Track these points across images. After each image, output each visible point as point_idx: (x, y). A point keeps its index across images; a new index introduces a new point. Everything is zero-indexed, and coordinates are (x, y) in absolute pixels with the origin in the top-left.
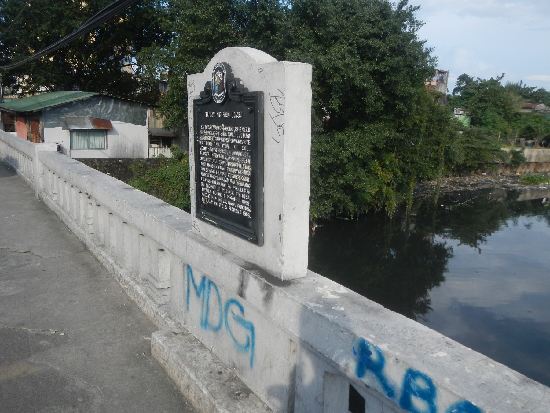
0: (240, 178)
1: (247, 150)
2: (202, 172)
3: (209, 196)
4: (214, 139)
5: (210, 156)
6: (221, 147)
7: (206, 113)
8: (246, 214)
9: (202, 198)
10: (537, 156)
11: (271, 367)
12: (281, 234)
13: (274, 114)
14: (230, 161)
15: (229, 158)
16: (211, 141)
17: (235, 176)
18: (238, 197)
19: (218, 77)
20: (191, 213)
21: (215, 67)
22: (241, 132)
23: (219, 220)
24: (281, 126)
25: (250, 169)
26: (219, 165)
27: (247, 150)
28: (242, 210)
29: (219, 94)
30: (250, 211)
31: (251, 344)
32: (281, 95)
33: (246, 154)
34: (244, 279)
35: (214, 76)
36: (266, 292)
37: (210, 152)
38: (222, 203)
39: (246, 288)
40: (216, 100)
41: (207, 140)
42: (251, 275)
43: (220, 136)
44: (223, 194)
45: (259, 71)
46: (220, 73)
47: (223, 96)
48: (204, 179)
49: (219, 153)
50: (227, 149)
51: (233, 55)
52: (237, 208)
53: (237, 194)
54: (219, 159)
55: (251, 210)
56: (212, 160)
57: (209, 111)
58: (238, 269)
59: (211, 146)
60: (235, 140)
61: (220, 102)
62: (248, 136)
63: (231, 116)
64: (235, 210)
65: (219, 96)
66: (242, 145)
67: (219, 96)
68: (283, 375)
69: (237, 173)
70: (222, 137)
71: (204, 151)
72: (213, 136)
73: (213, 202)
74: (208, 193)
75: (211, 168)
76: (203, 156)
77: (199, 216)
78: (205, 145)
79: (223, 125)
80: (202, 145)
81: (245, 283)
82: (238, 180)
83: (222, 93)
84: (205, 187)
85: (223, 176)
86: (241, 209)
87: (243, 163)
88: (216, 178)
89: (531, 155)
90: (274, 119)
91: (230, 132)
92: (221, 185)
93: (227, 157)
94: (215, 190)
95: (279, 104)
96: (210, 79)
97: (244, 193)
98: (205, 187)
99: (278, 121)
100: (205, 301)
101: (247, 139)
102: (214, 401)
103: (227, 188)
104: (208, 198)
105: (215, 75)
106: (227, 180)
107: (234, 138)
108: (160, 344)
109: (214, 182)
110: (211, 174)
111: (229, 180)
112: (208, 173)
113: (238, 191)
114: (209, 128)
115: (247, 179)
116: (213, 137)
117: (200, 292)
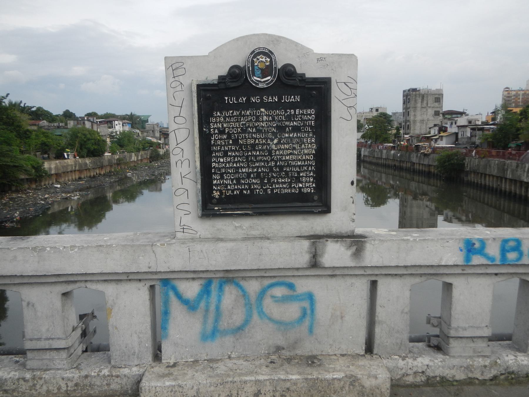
0: (294, 157)
1: (310, 130)
3: (229, 187)
6: (259, 131)
8: (305, 191)
9: (214, 192)
10: (56, 168)
11: (342, 317)
12: (354, 197)
13: (342, 97)
15: (275, 141)
16: (237, 128)
17: (287, 158)
18: (294, 177)
19: (262, 61)
21: (253, 51)
22: (298, 115)
23: (252, 208)
24: (353, 107)
25: (315, 147)
26: (257, 151)
28: (300, 188)
29: (262, 78)
30: (314, 185)
31: (309, 312)
32: (352, 81)
34: (317, 248)
35: (253, 62)
36: (354, 249)
37: (233, 140)
39: (322, 255)
41: (229, 128)
42: (329, 242)
44: (262, 180)
45: (320, 59)
46: (264, 57)
47: (272, 81)
48: (220, 171)
49: (255, 139)
50: (273, 133)
51: (272, 41)
52: (290, 187)
54: (253, 146)
55: (315, 184)
58: (306, 244)
63: (280, 99)
68: (360, 315)
69: (291, 154)
70: (263, 121)
72: (241, 122)
81: (319, 252)
83: (269, 78)
84: (222, 178)
85: (264, 161)
87: (301, 143)
88: (248, 165)
89: (51, 167)
90: (342, 101)
93: (272, 140)
94: (243, 179)
95: (350, 88)
99: (349, 103)
100: (212, 308)
101: (312, 120)
102: (314, 376)
105: (255, 60)
107: (286, 121)
108: (169, 387)
109: (244, 170)
110: (239, 161)
112: (229, 162)
114: (233, 113)
115: (311, 157)
117: (198, 304)
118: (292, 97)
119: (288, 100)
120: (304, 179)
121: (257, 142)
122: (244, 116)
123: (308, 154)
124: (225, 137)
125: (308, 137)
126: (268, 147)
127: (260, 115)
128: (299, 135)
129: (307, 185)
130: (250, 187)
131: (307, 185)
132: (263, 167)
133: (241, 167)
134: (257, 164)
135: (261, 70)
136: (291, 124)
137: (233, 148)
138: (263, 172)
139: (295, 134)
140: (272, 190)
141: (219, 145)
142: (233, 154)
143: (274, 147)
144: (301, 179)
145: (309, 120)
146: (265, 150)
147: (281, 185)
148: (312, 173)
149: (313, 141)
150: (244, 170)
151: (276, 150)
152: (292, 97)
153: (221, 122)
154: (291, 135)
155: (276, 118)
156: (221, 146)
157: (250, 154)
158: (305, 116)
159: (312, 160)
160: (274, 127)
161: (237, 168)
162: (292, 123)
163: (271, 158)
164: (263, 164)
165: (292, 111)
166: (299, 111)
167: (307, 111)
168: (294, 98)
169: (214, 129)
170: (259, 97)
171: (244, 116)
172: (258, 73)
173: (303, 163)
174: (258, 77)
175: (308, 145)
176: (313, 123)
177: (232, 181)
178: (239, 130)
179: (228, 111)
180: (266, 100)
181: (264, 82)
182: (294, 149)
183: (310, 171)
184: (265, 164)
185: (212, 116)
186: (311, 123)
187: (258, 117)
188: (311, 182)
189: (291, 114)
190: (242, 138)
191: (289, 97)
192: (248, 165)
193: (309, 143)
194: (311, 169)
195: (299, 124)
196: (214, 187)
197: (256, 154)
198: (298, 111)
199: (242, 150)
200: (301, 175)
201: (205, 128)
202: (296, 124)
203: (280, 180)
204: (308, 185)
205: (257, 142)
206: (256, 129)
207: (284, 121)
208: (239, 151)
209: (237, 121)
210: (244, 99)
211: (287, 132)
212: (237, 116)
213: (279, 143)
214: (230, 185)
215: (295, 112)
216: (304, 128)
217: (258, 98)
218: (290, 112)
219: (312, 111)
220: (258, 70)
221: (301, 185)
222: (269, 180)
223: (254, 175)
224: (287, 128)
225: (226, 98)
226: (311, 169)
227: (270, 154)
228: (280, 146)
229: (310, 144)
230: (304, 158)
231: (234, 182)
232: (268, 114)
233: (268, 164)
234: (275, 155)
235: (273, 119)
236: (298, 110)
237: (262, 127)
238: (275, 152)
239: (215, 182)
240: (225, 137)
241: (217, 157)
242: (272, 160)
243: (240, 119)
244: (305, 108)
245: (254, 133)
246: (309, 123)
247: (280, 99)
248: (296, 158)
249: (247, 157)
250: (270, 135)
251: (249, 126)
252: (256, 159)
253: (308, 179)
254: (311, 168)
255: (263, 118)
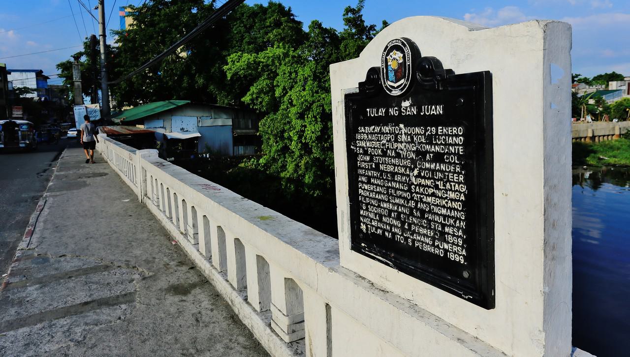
0: (438, 201)
1: (456, 162)
2: (360, 190)
3: (373, 224)
4: (384, 145)
5: (377, 168)
6: (398, 155)
7: (368, 110)
8: (452, 257)
9: (362, 224)
14: (419, 176)
15: (416, 172)
16: (377, 148)
17: (429, 199)
20: (337, 238)
22: (442, 135)
25: (464, 190)
26: (396, 181)
27: (456, 162)
28: (446, 251)
29: (396, 83)
30: (464, 253)
33: (455, 167)
35: (386, 59)
38: (402, 235)
40: (391, 91)
41: (371, 148)
43: (396, 141)
44: (403, 223)
47: (405, 85)
48: (365, 200)
49: (395, 165)
52: (433, 245)
53: (435, 225)
54: (393, 174)
56: (381, 175)
57: (370, 108)
59: (378, 155)
60: (428, 147)
61: (399, 94)
62: (460, 140)
64: (427, 248)
65: (396, 85)
66: (444, 154)
67: (395, 87)
69: (433, 195)
70: (401, 142)
71: (365, 161)
72: (381, 141)
73: (384, 233)
74: (373, 219)
75: (377, 185)
76: (362, 168)
77: (356, 247)
78: (366, 153)
79: (402, 126)
80: (361, 154)
82: (437, 205)
83: (402, 81)
84: (367, 209)
85: (405, 198)
86: (444, 249)
88: (389, 199)
91: (417, 134)
92: (400, 210)
93: (412, 170)
94: (385, 216)
96: (378, 63)
97: (450, 226)
98: (367, 209)
101: (459, 145)
103: (411, 214)
104: (370, 223)
106: (412, 204)
107: (426, 144)
109: (385, 205)
110: (379, 193)
111: (417, 204)
112: (372, 191)
113: (435, 221)
114: (374, 130)
116: (382, 143)
118: (433, 107)
119: (428, 112)
120: (450, 238)
121: (396, 170)
122: (383, 134)
123: (455, 200)
124: (368, 158)
125: (455, 172)
126: (408, 180)
127: (398, 134)
128: (442, 167)
129: (455, 249)
130: (391, 229)
131: (455, 249)
132: (404, 206)
133: (384, 201)
134: (397, 201)
135: (394, 70)
136: (432, 150)
137: (375, 175)
138: (403, 213)
139: (438, 164)
140: (413, 241)
141: (362, 168)
142: (376, 182)
143: (413, 179)
144: (446, 236)
145: (456, 144)
146: (404, 183)
147: (422, 237)
148: (460, 231)
149: (461, 179)
150: (385, 205)
151: (416, 186)
152: (433, 107)
153: (365, 140)
154: (433, 166)
155: (415, 139)
156: (366, 169)
157: (390, 185)
158: (450, 138)
159: (460, 211)
160: (414, 152)
161: (379, 201)
162: (433, 147)
163: (411, 195)
164: (403, 202)
165: (434, 130)
166: (442, 129)
167: (452, 129)
168: (436, 108)
169: (360, 147)
170: (397, 108)
171: (383, 134)
172: (391, 75)
173: (449, 213)
174: (392, 82)
175: (455, 186)
176: (460, 150)
177: (376, 214)
178: (380, 152)
179: (370, 126)
180: (404, 113)
181: (398, 87)
182: (437, 187)
183: (459, 228)
184: (404, 202)
185: (357, 132)
186: (458, 149)
187: (396, 135)
188: (459, 246)
189: (432, 134)
190: (382, 163)
191: (430, 107)
192: (389, 199)
193: (456, 182)
194: (460, 224)
195: (443, 149)
196: (361, 219)
197: (396, 186)
198: (440, 129)
199: (383, 179)
200: (447, 230)
201: (353, 146)
202: (439, 150)
203: (422, 231)
204: (456, 250)
205: (396, 170)
206: (396, 152)
207: (423, 143)
208: (379, 179)
209: (378, 140)
210: (384, 111)
211: (428, 161)
212: (378, 133)
213: (419, 176)
214: (374, 220)
215: (437, 131)
216: (449, 158)
217: (396, 110)
218: (431, 131)
219: (460, 130)
220: (391, 71)
221: (446, 246)
222: (409, 225)
223: (394, 215)
224: (428, 155)
225: (368, 110)
226: (460, 224)
227: (409, 190)
228: (420, 180)
229: (457, 185)
230: (449, 205)
231: (378, 218)
232: (406, 132)
233: (408, 203)
234: (417, 193)
235: (412, 141)
236: (441, 128)
237: (401, 150)
238: (415, 189)
239: (362, 212)
240: (368, 158)
241: (363, 182)
242: (412, 199)
243: (380, 137)
244: (452, 126)
245: (393, 157)
246: (455, 149)
247: (419, 110)
248: (440, 203)
249: (388, 188)
250: (408, 163)
251: (388, 148)
252: (396, 193)
253: (455, 239)
254: (460, 223)
255: (401, 138)
